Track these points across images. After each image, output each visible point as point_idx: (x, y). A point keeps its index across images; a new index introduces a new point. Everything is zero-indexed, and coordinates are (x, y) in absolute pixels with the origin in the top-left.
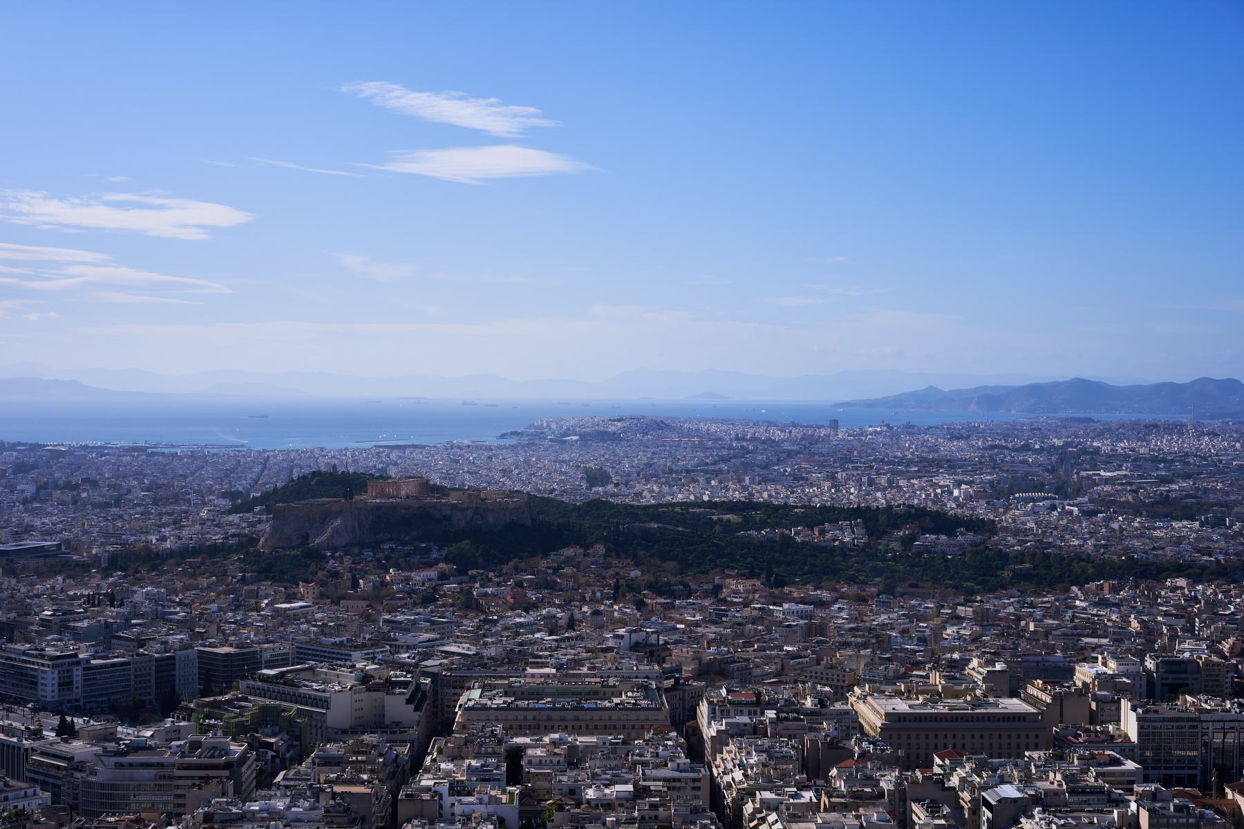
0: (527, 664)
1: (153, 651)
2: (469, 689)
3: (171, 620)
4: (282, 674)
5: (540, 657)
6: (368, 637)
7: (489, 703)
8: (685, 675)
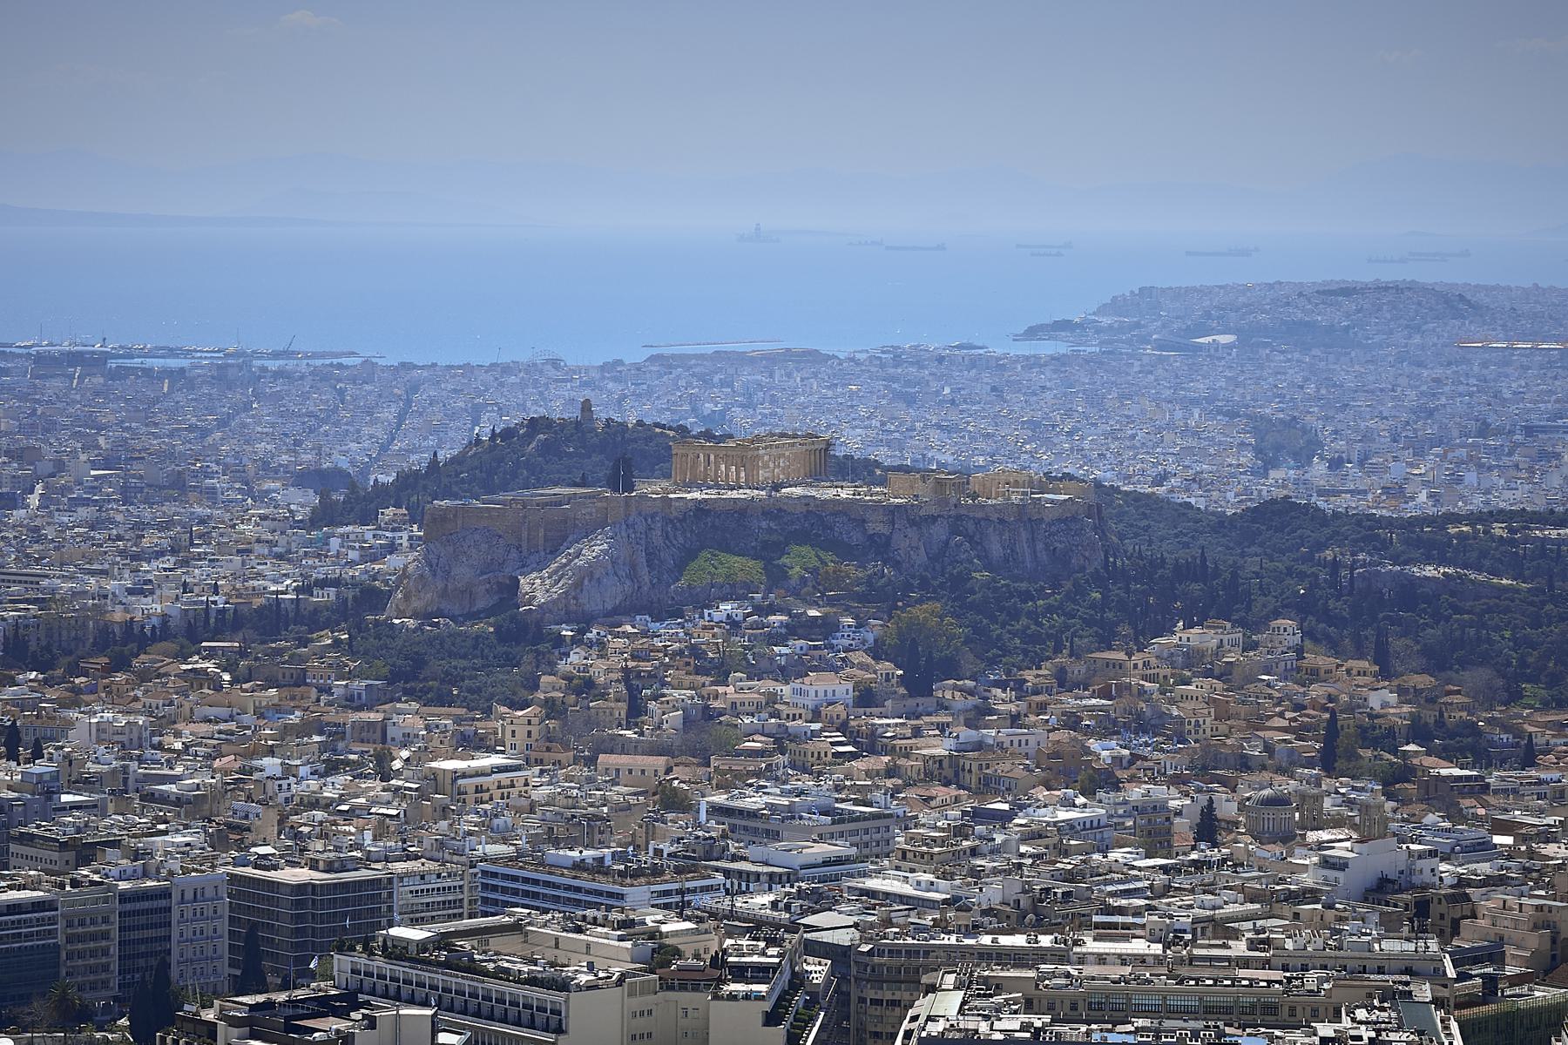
0: (1088, 925)
1: (114, 874)
2: (932, 989)
3: (164, 799)
4: (443, 941)
5: (1121, 911)
6: (667, 848)
7: (984, 1027)
8: (1510, 970)
